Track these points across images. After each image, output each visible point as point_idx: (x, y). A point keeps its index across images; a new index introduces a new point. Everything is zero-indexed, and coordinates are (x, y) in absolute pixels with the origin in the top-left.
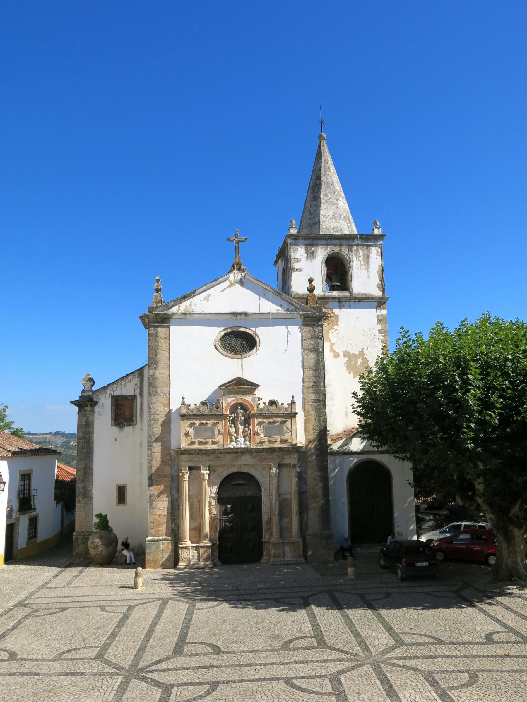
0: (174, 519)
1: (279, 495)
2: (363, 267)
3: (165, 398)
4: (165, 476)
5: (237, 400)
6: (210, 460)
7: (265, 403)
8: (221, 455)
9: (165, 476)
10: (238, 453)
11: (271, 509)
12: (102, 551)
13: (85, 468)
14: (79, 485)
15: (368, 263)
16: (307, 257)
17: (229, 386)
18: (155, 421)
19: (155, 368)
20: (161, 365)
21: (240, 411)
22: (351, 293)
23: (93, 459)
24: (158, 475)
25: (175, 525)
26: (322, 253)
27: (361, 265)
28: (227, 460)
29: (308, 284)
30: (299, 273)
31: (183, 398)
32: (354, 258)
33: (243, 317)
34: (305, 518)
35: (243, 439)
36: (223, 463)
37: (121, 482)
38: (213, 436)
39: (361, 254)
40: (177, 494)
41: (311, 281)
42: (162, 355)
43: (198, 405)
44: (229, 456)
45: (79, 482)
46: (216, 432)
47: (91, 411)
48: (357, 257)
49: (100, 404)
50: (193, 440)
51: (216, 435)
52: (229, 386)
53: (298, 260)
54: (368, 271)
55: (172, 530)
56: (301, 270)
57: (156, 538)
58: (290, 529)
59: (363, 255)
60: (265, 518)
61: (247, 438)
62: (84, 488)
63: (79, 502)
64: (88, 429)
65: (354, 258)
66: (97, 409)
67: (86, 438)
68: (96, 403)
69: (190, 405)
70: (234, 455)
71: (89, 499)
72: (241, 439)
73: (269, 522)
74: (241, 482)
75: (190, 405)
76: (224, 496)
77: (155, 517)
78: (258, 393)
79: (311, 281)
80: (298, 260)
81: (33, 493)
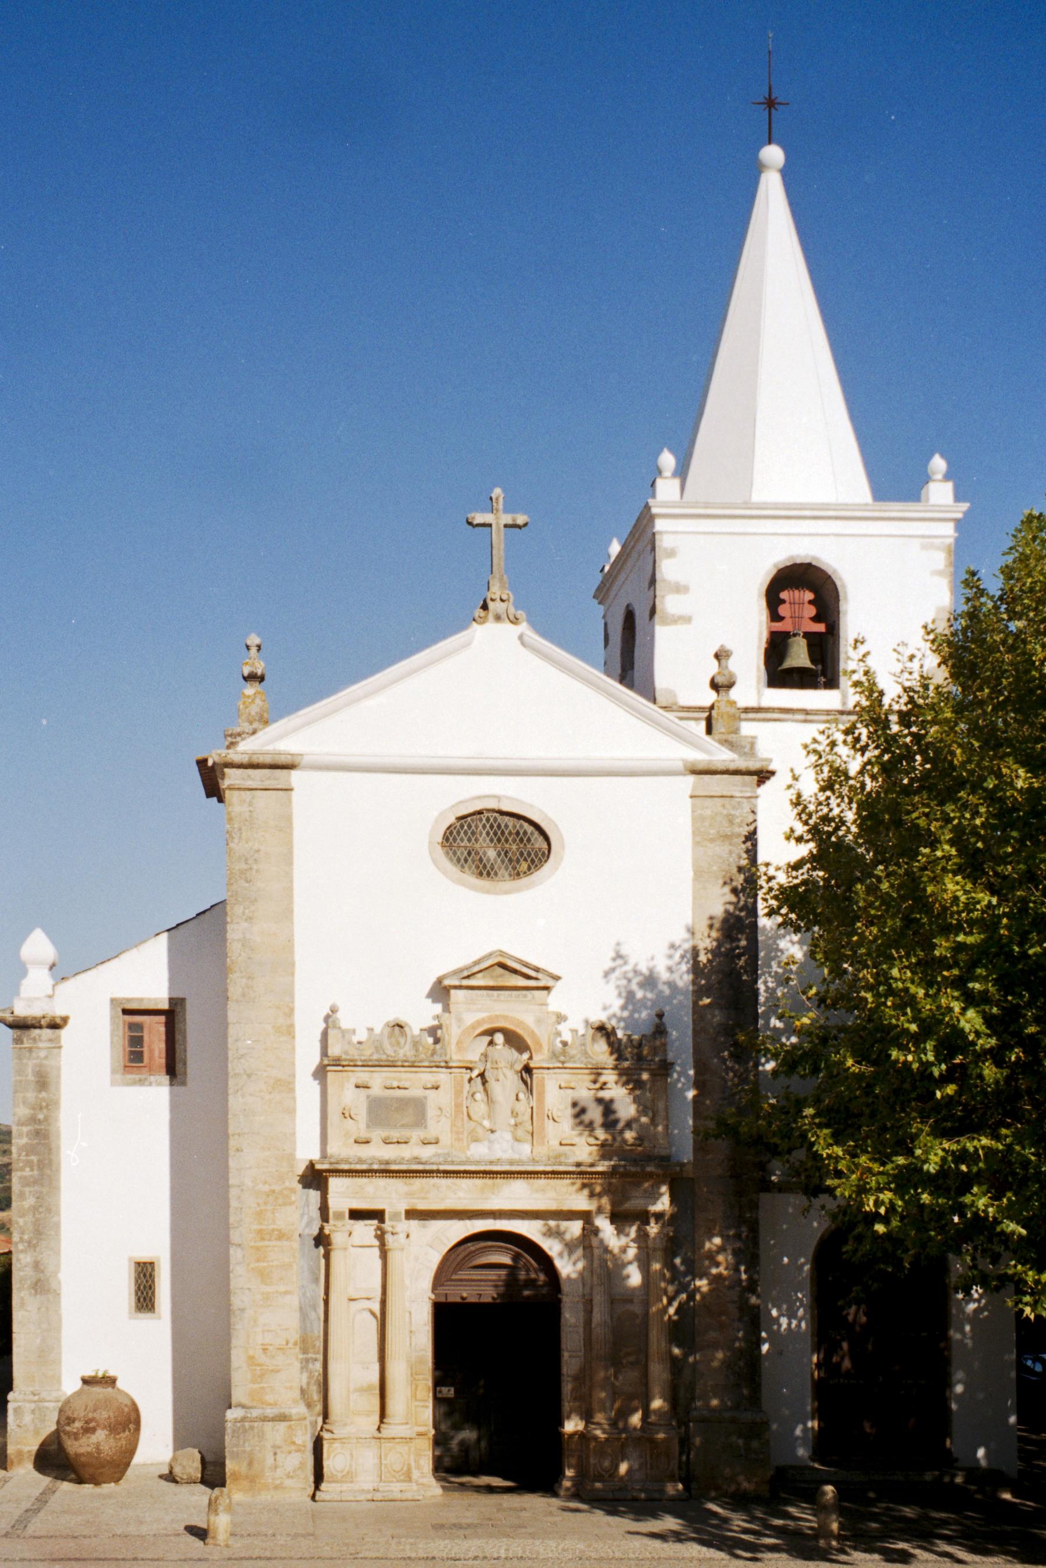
0: (307, 1360)
3: (278, 1008)
4: (281, 1236)
5: (490, 1019)
6: (409, 1195)
7: (574, 1031)
9: (281, 1236)
11: (588, 1342)
12: (98, 1446)
13: (35, 1209)
14: (21, 1256)
17: (468, 977)
18: (249, 1076)
23: (58, 1180)
24: (260, 1232)
25: (310, 1377)
29: (712, 668)
35: (508, 1136)
37: (144, 1256)
40: (314, 1286)
43: (378, 1030)
45: (21, 1247)
46: (431, 1112)
47: (50, 1040)
50: (364, 1135)
51: (431, 1123)
52: (468, 977)
53: (680, 589)
55: (303, 1391)
56: (687, 620)
57: (255, 1413)
60: (570, 1363)
61: (520, 1133)
62: (37, 1265)
63: (22, 1304)
64: (44, 1094)
67: (40, 1122)
69: (354, 1032)
70: (478, 1182)
71: (50, 1296)
72: (505, 1136)
75: (354, 1032)
76: (451, 1299)
77: (251, 1353)
78: (555, 1001)
80: (680, 589)
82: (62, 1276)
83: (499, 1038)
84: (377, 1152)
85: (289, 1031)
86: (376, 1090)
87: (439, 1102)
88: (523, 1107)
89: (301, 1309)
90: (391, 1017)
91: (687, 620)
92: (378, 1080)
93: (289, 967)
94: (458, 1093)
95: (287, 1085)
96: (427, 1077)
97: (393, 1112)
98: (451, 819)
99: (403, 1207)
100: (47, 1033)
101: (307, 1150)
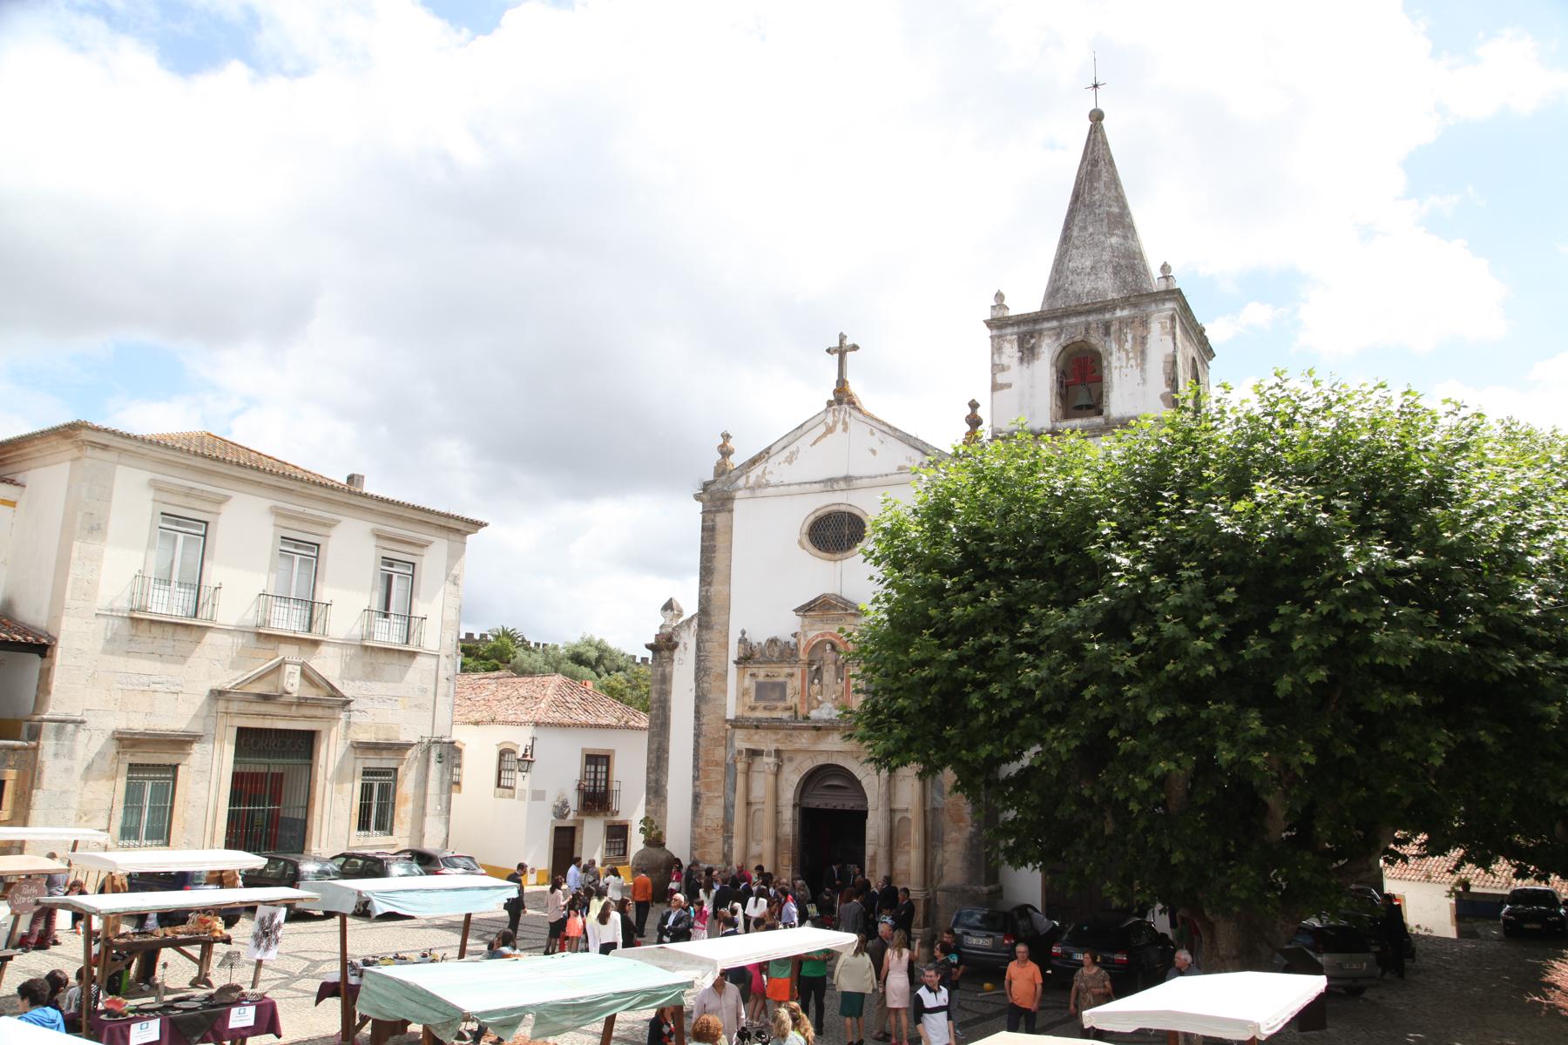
1: (892, 811)
2: (1132, 362)
4: (717, 764)
6: (777, 741)
8: (795, 733)
9: (717, 764)
10: (820, 729)
15: (1143, 352)
16: (1021, 360)
19: (710, 584)
20: (717, 578)
21: (829, 655)
22: (1107, 418)
26: (1048, 350)
27: (1128, 358)
28: (804, 740)
29: (968, 411)
30: (1006, 391)
31: (743, 633)
32: (1114, 347)
33: (842, 485)
34: (939, 858)
36: (797, 746)
38: (783, 697)
39: (1129, 337)
41: (974, 405)
42: (719, 564)
44: (806, 734)
46: (789, 691)
48: (1121, 343)
49: (681, 646)
51: (789, 697)
53: (1003, 369)
54: (1143, 370)
56: (1010, 386)
58: (907, 874)
59: (1134, 338)
60: (869, 850)
65: (1114, 347)
66: (677, 654)
68: (676, 646)
73: (873, 859)
74: (836, 783)
79: (974, 405)
80: (1003, 369)
81: (615, 786)
82: (669, 787)
83: (828, 647)
84: (760, 714)
85: (726, 646)
86: (761, 679)
87: (795, 684)
88: (839, 688)
89: (725, 808)
90: (771, 635)
91: (1010, 386)
92: (762, 673)
93: (727, 609)
94: (803, 679)
95: (723, 676)
96: (788, 670)
97: (768, 691)
98: (812, 518)
99: (773, 747)
100: (666, 653)
101: (730, 715)
